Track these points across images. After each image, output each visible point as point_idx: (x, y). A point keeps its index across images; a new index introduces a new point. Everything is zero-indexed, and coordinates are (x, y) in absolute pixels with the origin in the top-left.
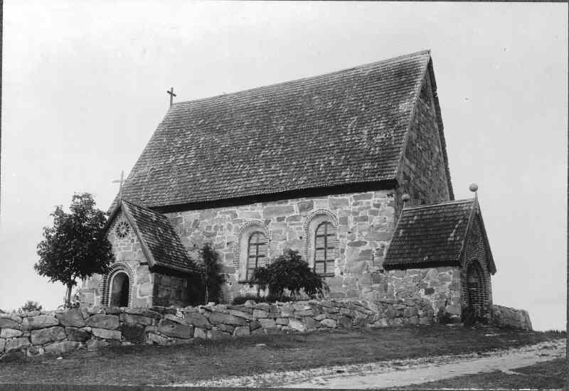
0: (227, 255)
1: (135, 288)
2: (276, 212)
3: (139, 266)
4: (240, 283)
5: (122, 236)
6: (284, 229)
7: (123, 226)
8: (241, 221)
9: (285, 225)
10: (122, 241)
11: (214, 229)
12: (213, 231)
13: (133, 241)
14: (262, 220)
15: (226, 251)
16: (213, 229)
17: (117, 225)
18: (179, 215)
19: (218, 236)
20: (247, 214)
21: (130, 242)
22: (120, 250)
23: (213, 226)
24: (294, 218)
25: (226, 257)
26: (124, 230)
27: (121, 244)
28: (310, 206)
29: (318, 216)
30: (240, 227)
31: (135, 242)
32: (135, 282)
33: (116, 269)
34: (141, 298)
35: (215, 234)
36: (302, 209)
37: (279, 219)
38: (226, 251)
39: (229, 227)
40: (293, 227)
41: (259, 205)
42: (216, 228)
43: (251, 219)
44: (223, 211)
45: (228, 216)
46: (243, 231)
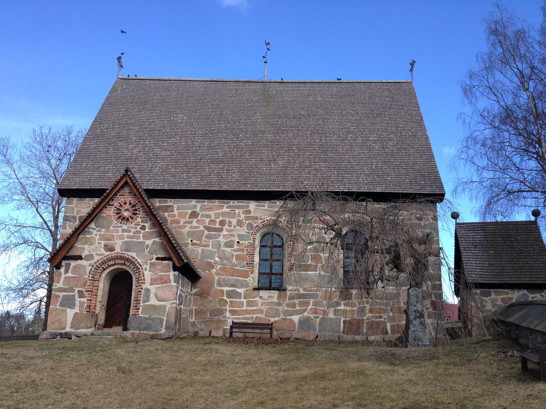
0: (237, 255)
1: (148, 291)
3: (154, 260)
4: (254, 289)
7: (127, 206)
8: (257, 218)
10: (125, 227)
11: (220, 225)
12: (217, 226)
13: (143, 228)
15: (235, 251)
16: (218, 224)
17: (116, 204)
18: (170, 202)
19: (225, 232)
21: (138, 229)
22: (121, 237)
23: (218, 220)
25: (236, 258)
26: (126, 214)
27: (123, 231)
30: (255, 225)
31: (147, 230)
33: (112, 263)
34: (158, 303)
35: (221, 230)
38: (235, 251)
42: (222, 223)
44: (231, 204)
45: (237, 211)
46: (258, 228)
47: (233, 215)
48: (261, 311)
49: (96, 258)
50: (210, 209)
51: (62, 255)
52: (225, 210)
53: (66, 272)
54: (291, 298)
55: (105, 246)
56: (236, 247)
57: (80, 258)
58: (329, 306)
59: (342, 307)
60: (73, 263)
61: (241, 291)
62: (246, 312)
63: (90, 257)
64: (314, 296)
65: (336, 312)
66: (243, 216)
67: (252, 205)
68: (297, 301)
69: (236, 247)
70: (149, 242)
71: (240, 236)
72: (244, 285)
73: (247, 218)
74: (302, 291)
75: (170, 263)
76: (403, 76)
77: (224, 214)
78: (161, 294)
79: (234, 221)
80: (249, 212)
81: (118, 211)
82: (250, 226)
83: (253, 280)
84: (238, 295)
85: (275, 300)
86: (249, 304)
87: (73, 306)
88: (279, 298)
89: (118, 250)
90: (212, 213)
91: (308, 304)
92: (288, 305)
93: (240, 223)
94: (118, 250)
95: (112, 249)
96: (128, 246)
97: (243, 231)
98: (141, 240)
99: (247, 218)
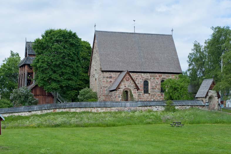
2: (153, 76)
5: (127, 81)
6: (155, 81)
7: (127, 78)
8: (144, 78)
9: (155, 80)
12: (136, 79)
13: (131, 82)
14: (149, 78)
19: (137, 81)
20: (145, 76)
23: (136, 78)
24: (158, 78)
28: (161, 76)
29: (163, 78)
32: (133, 93)
35: (136, 80)
36: (159, 76)
37: (154, 78)
39: (140, 79)
40: (158, 81)
41: (148, 74)
42: (137, 78)
43: (146, 77)
45: (140, 76)
47: (138, 77)
48: (145, 98)
49: (123, 88)
50: (134, 75)
51: (118, 88)
52: (137, 75)
53: (118, 91)
54: (151, 95)
55: (125, 86)
56: (140, 84)
57: (120, 88)
58: (159, 97)
59: (161, 97)
60: (119, 89)
61: (141, 94)
62: (142, 98)
63: (122, 88)
64: (156, 95)
65: (160, 98)
66: (141, 77)
67: (143, 74)
68: (152, 96)
69: (140, 84)
70: (132, 85)
71: (141, 82)
72: (142, 93)
73: (142, 77)
74: (153, 94)
75: (136, 89)
76: (169, 33)
77: (137, 76)
78: (135, 95)
79: (139, 78)
80: (142, 76)
81: (126, 79)
82: (142, 79)
83: (143, 91)
84: (141, 95)
85: (148, 96)
86: (143, 97)
87: (120, 98)
88: (149, 95)
89: (127, 87)
90: (134, 76)
91: (155, 96)
92: (151, 97)
93: (140, 79)
94: (127, 87)
95: (126, 87)
96: (128, 86)
97: (141, 80)
98: (131, 85)
99: (142, 77)
